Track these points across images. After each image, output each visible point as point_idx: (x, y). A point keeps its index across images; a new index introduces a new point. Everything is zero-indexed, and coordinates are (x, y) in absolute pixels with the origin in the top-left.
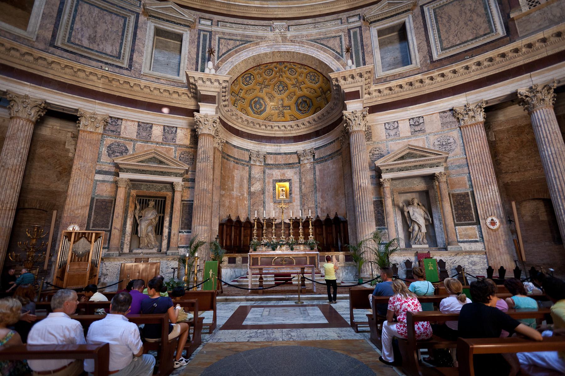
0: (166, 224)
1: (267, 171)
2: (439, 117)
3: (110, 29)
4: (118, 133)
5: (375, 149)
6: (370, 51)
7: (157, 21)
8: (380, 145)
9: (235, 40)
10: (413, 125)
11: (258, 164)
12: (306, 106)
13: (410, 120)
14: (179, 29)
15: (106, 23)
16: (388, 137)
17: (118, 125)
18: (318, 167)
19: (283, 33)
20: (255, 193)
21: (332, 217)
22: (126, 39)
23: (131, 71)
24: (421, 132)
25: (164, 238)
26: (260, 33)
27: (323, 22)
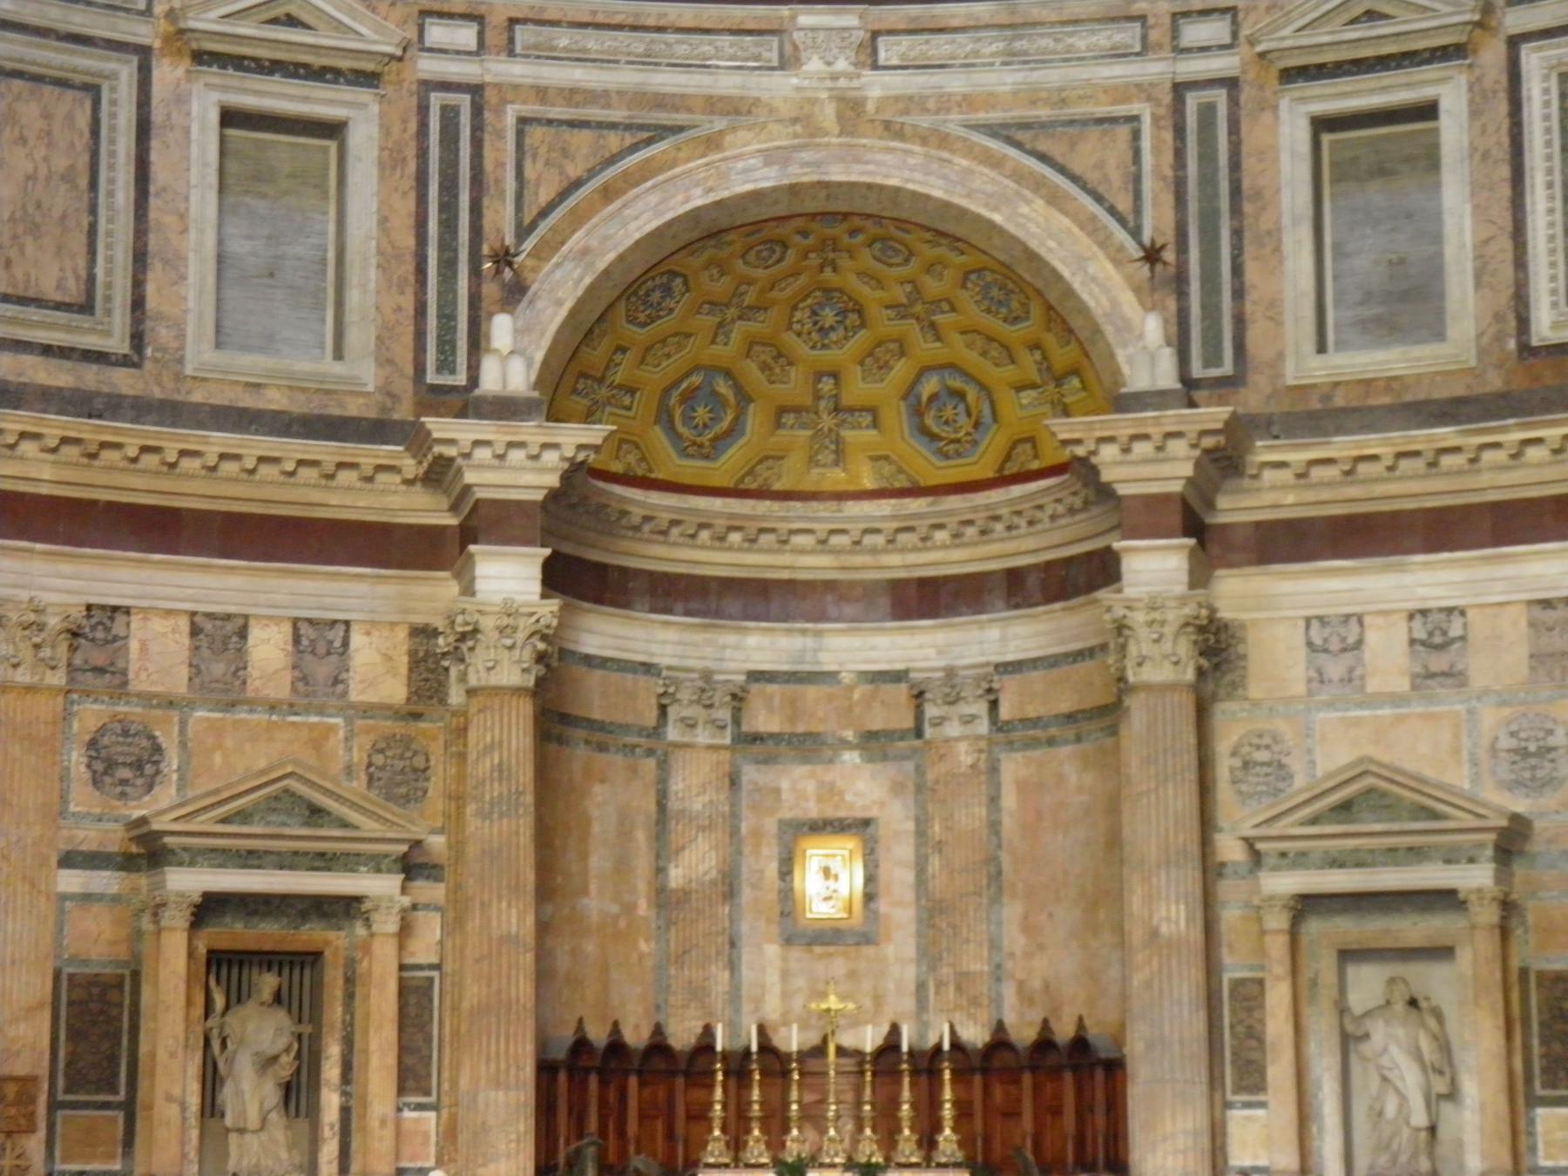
0: (331, 1071)
1: (751, 774)
2: (1523, 623)
3: (43, 172)
4: (117, 680)
5: (1255, 741)
6: (1269, 233)
7: (232, 77)
8: (1281, 726)
9: (600, 125)
10: (1423, 643)
11: (703, 737)
12: (963, 420)
13: (1411, 617)
14: (331, 102)
15: (23, 140)
16: (1315, 685)
17: (116, 639)
18: (1013, 767)
19: (842, 83)
20: (685, 894)
21: (1064, 1032)
22: (111, 207)
23: (137, 365)
24: (1450, 681)
25: (327, 1132)
26: (727, 84)
27: (1053, 24)
